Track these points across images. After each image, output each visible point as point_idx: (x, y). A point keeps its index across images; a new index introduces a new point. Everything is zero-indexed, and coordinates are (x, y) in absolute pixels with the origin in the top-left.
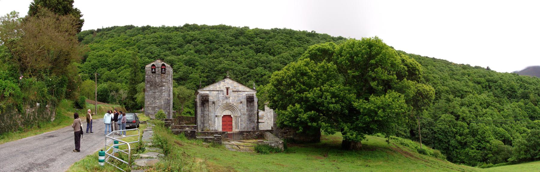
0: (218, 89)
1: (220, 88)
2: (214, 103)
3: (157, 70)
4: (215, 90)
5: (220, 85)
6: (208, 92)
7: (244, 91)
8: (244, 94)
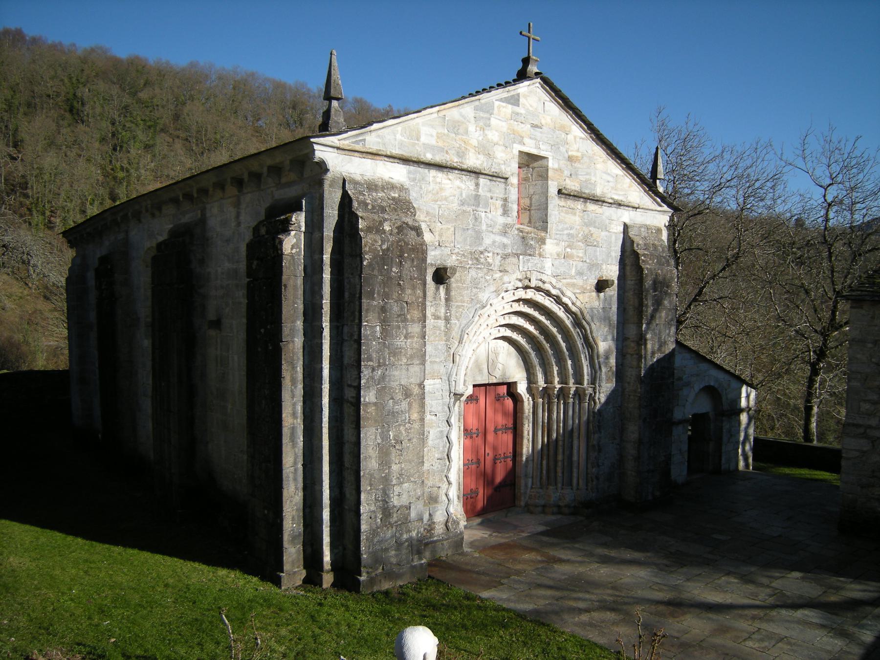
0: (473, 161)
1: (485, 150)
2: (441, 276)
4: (454, 160)
6: (397, 173)
7: (619, 204)
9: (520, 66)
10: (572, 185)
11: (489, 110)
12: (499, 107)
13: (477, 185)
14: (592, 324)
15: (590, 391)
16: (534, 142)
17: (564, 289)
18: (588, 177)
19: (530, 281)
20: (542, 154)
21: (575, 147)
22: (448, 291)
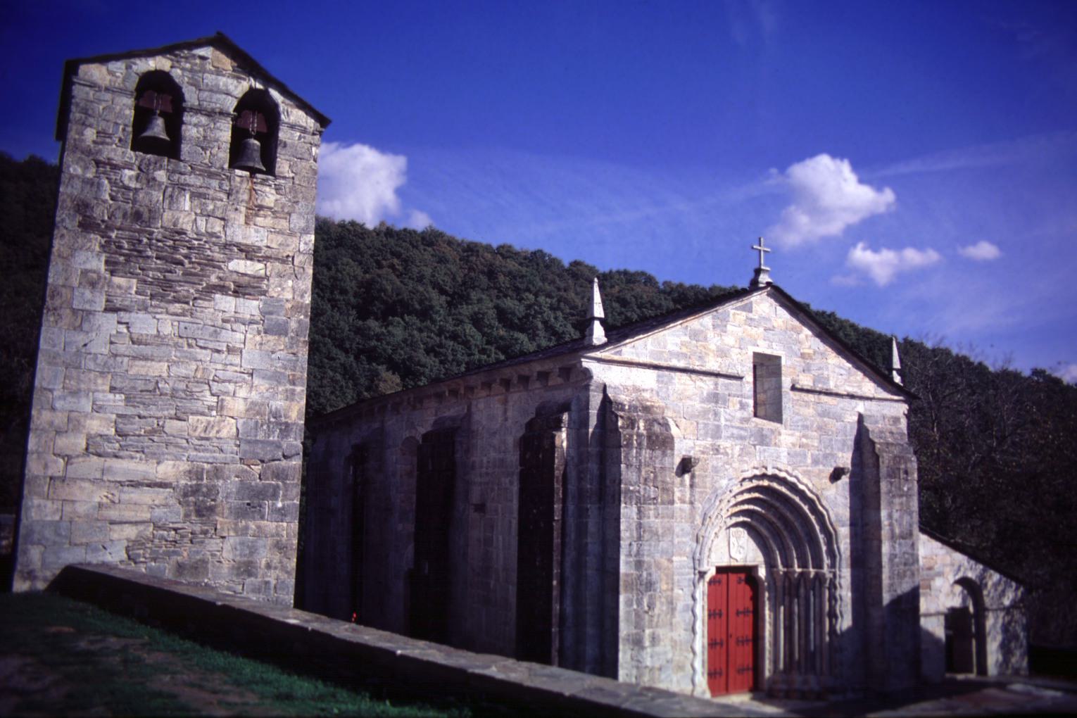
0: (712, 365)
1: (722, 353)
3: (192, 128)
6: (647, 379)
7: (852, 396)
9: (752, 275)
10: (806, 381)
11: (725, 320)
12: (734, 314)
13: (716, 384)
14: (830, 510)
15: (831, 576)
16: (767, 342)
17: (800, 477)
18: (820, 372)
19: (766, 468)
20: (775, 353)
21: (807, 344)
22: (693, 477)
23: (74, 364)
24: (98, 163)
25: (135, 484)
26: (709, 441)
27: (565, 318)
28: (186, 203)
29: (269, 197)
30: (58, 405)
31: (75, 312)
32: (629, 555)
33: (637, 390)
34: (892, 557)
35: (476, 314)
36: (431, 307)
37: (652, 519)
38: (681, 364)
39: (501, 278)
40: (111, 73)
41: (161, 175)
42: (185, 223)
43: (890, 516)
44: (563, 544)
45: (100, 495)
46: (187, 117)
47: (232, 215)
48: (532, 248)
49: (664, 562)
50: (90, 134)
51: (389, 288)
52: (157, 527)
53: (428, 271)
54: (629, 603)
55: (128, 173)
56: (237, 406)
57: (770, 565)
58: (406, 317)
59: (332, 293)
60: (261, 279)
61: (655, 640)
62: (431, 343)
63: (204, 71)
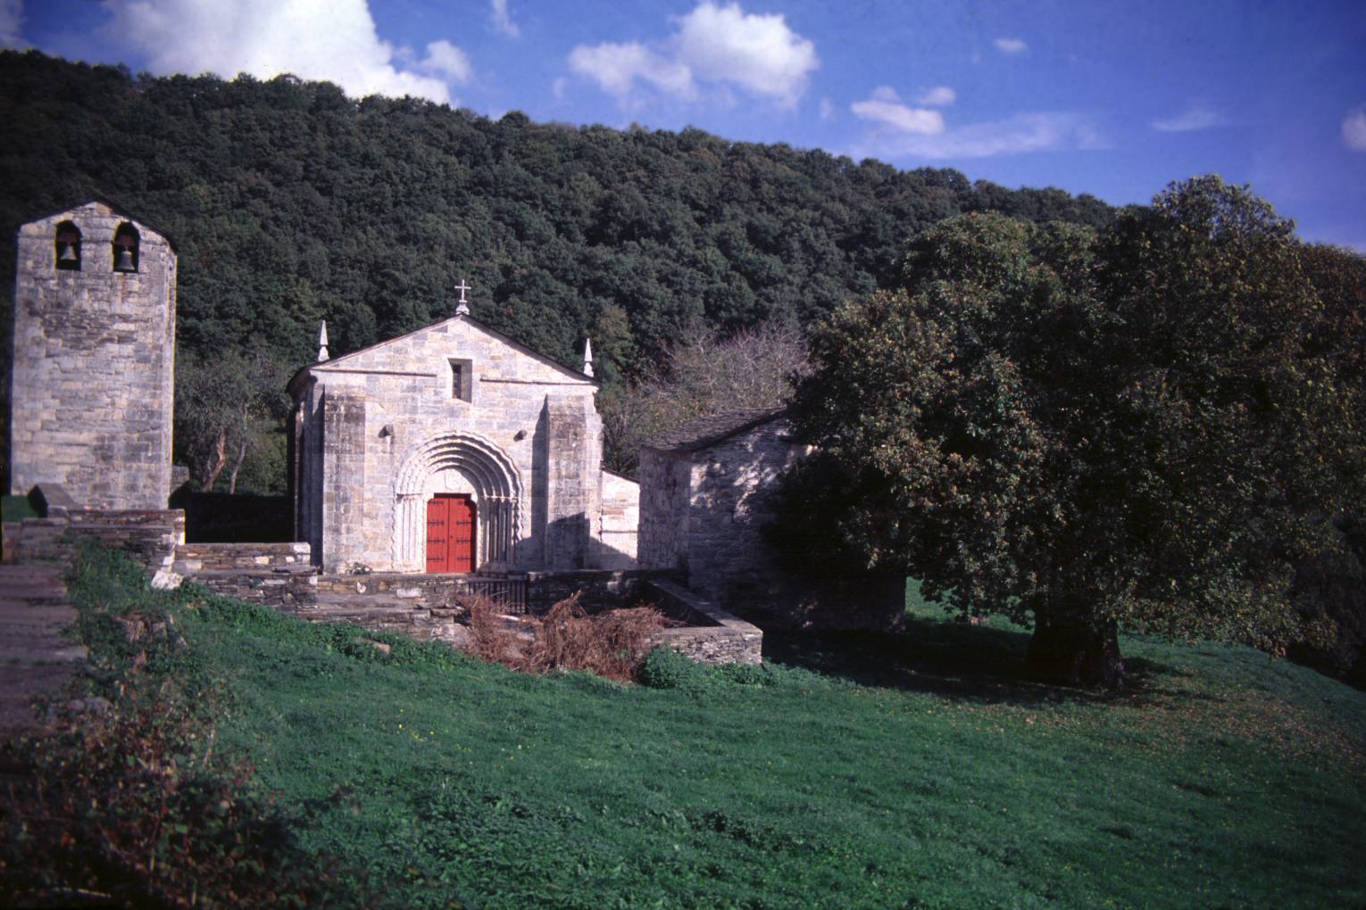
0: (411, 368)
1: (420, 360)
3: (87, 251)
5: (422, 345)
6: (360, 380)
8: (537, 396)
20: (467, 357)
22: (393, 438)
23: (32, 385)
24: (36, 279)
25: (69, 445)
26: (408, 416)
27: (829, 236)
28: (86, 295)
29: (135, 285)
30: (26, 406)
31: (30, 359)
32: (330, 482)
33: (346, 387)
34: (558, 491)
35: (723, 234)
36: (672, 228)
37: (347, 462)
38: (386, 370)
39: (765, 186)
40: (39, 227)
41: (71, 281)
42: (86, 306)
43: (558, 463)
44: (301, 476)
45: (50, 451)
46: (83, 246)
47: (113, 298)
48: (810, 146)
49: (356, 486)
50: (30, 264)
51: (627, 206)
52: (82, 466)
53: (677, 184)
54: (330, 509)
55: (52, 282)
56: (123, 401)
57: (480, 494)
58: (643, 241)
59: (563, 214)
60: (133, 332)
61: (349, 530)
62: (666, 270)
63: (92, 217)
